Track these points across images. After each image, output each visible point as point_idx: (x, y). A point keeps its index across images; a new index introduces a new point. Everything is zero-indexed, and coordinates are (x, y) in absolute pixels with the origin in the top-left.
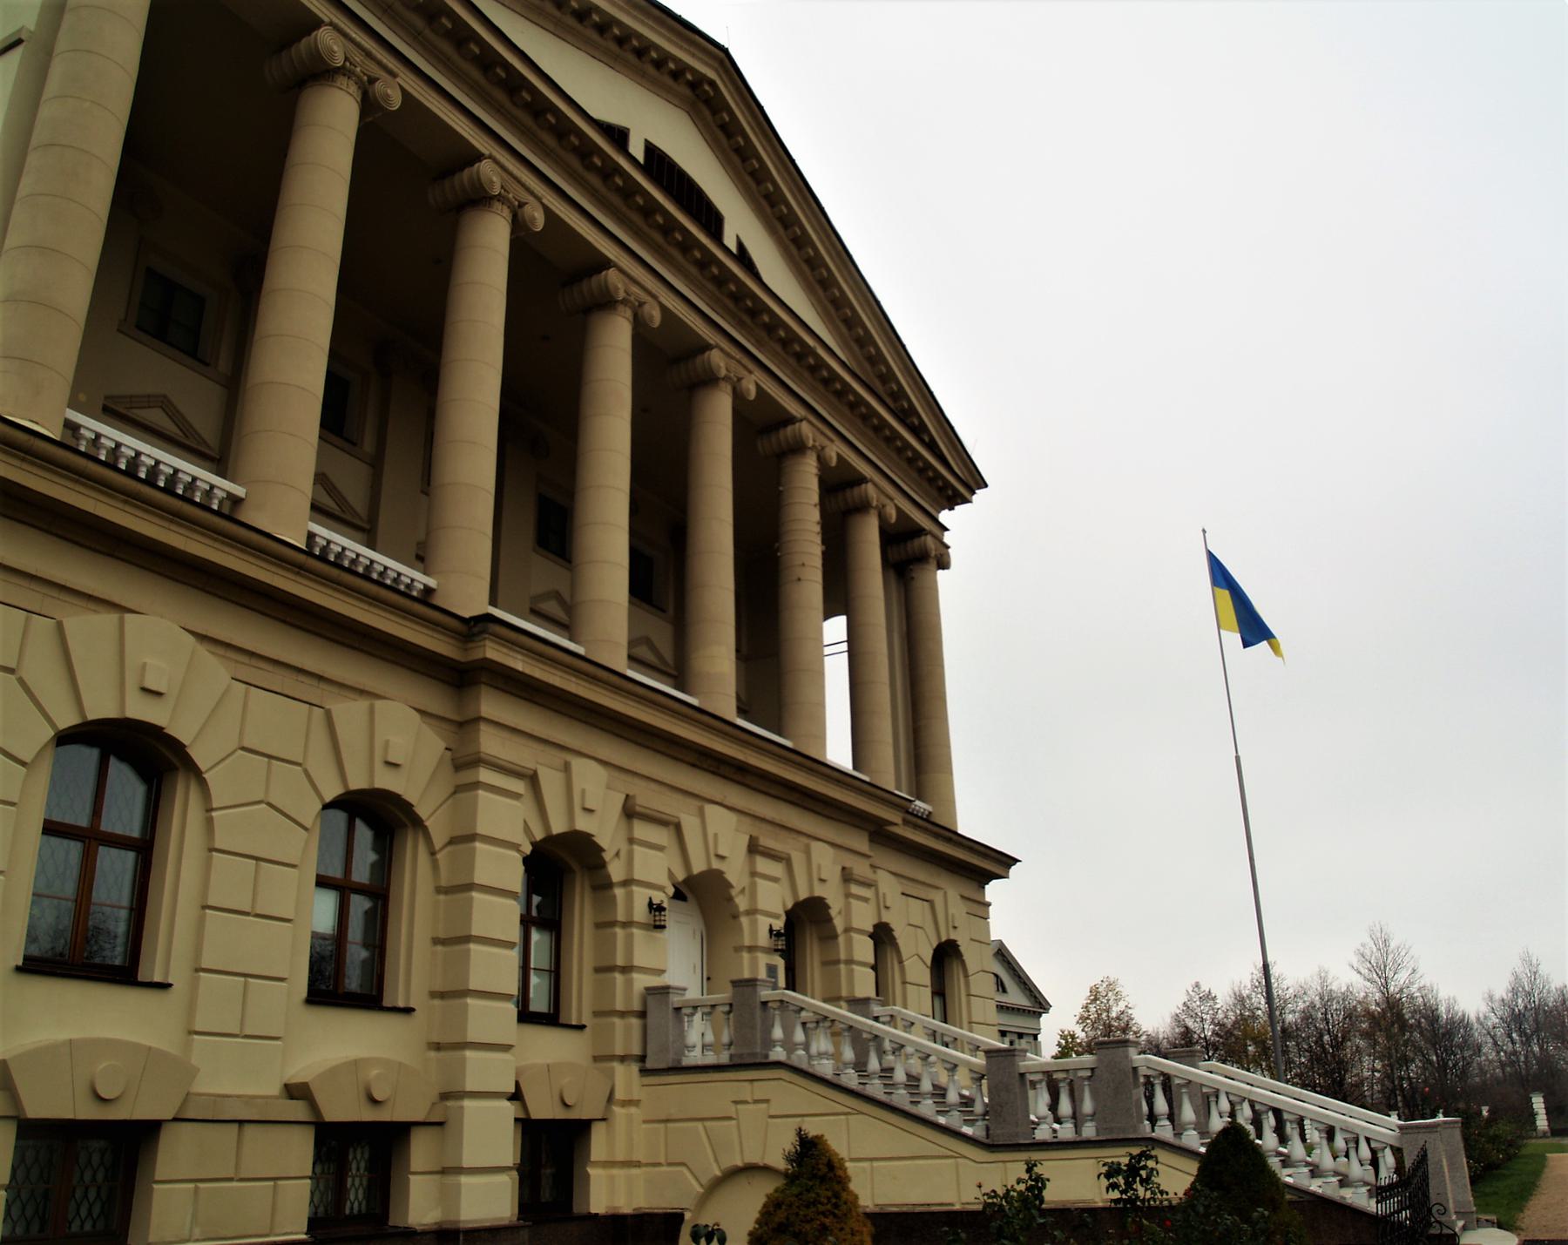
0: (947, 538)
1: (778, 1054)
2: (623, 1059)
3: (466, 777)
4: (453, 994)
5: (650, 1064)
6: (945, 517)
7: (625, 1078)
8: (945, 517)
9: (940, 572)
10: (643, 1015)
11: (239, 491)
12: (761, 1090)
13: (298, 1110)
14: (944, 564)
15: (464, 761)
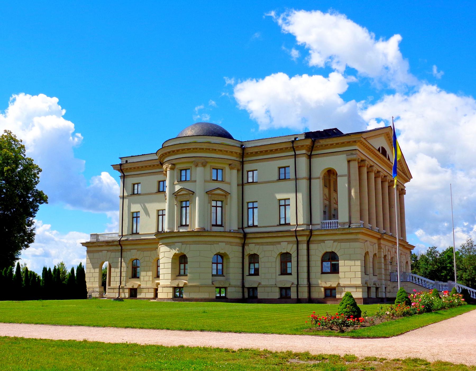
0: (406, 189)
1: (408, 280)
2: (388, 280)
3: (379, 250)
4: (380, 274)
5: (391, 281)
6: (406, 185)
7: (389, 282)
8: (406, 185)
9: (404, 195)
10: (390, 275)
11: (364, 222)
12: (406, 284)
13: (375, 286)
14: (405, 194)
15: (380, 248)
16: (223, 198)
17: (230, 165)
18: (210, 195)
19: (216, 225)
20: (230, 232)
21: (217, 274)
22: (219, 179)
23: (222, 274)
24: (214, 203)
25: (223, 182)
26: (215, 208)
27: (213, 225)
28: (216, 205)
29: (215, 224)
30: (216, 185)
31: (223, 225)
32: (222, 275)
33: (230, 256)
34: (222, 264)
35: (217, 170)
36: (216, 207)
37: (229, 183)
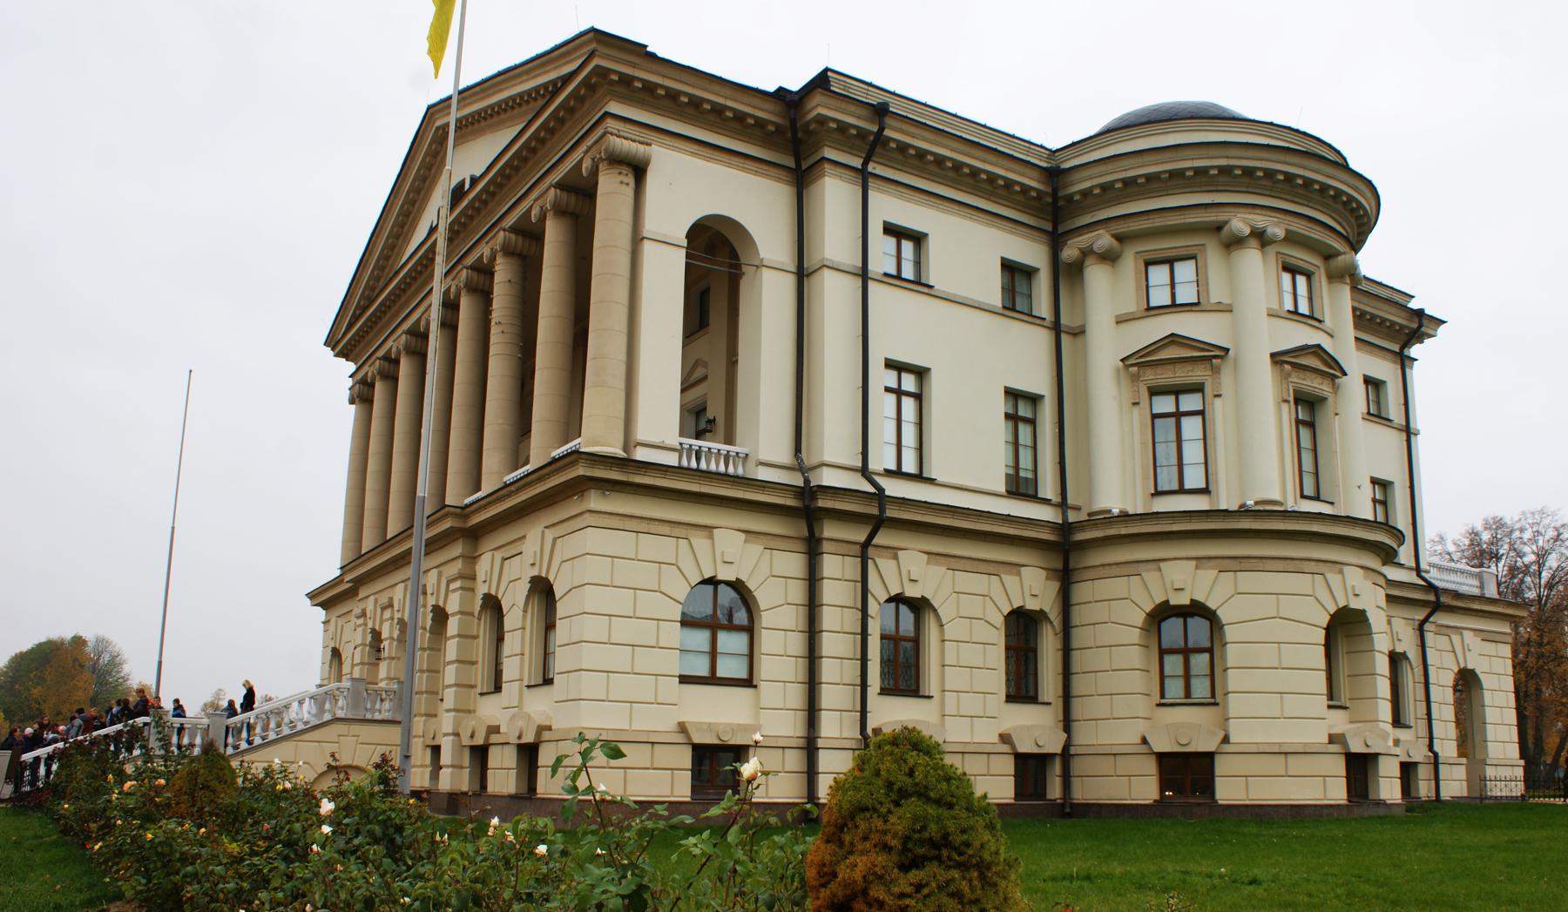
16: (1196, 374)
17: (1218, 228)
18: (1135, 369)
19: (1182, 490)
21: (1188, 694)
22: (1186, 294)
23: (1213, 695)
24: (1165, 404)
25: (1194, 308)
26: (1173, 420)
27: (1158, 493)
28: (1172, 409)
29: (1175, 487)
31: (1211, 488)
32: (1212, 701)
34: (1210, 651)
35: (1170, 262)
36: (1178, 415)
37: (1228, 310)
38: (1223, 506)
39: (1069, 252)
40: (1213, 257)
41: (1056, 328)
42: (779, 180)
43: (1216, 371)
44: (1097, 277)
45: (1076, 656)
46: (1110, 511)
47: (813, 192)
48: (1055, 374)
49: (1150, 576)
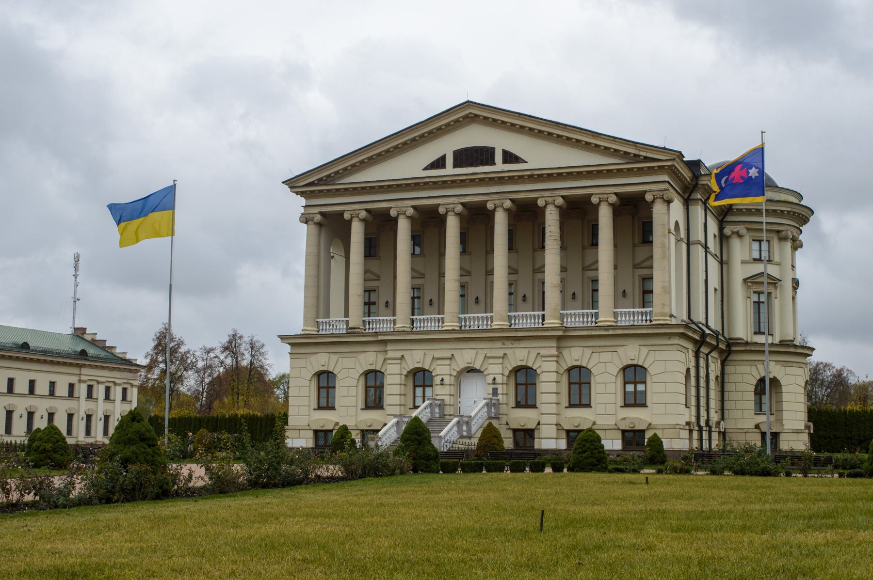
17: (778, 232)
18: (749, 284)
20: (782, 343)
22: (765, 254)
30: (759, 268)
33: (782, 382)
37: (778, 264)
38: (777, 341)
39: (727, 231)
40: (775, 243)
41: (721, 263)
42: (680, 201)
43: (776, 288)
44: (735, 243)
45: (726, 394)
46: (742, 339)
47: (691, 208)
48: (720, 280)
49: (760, 367)
